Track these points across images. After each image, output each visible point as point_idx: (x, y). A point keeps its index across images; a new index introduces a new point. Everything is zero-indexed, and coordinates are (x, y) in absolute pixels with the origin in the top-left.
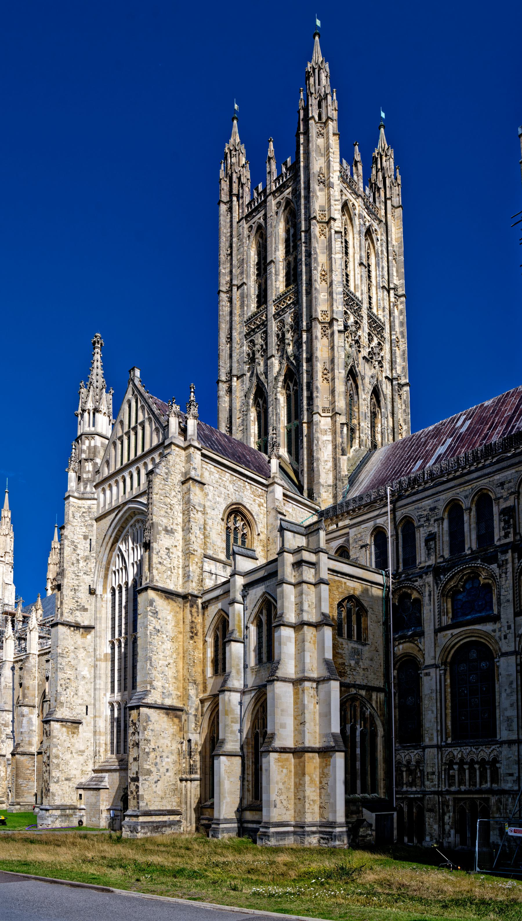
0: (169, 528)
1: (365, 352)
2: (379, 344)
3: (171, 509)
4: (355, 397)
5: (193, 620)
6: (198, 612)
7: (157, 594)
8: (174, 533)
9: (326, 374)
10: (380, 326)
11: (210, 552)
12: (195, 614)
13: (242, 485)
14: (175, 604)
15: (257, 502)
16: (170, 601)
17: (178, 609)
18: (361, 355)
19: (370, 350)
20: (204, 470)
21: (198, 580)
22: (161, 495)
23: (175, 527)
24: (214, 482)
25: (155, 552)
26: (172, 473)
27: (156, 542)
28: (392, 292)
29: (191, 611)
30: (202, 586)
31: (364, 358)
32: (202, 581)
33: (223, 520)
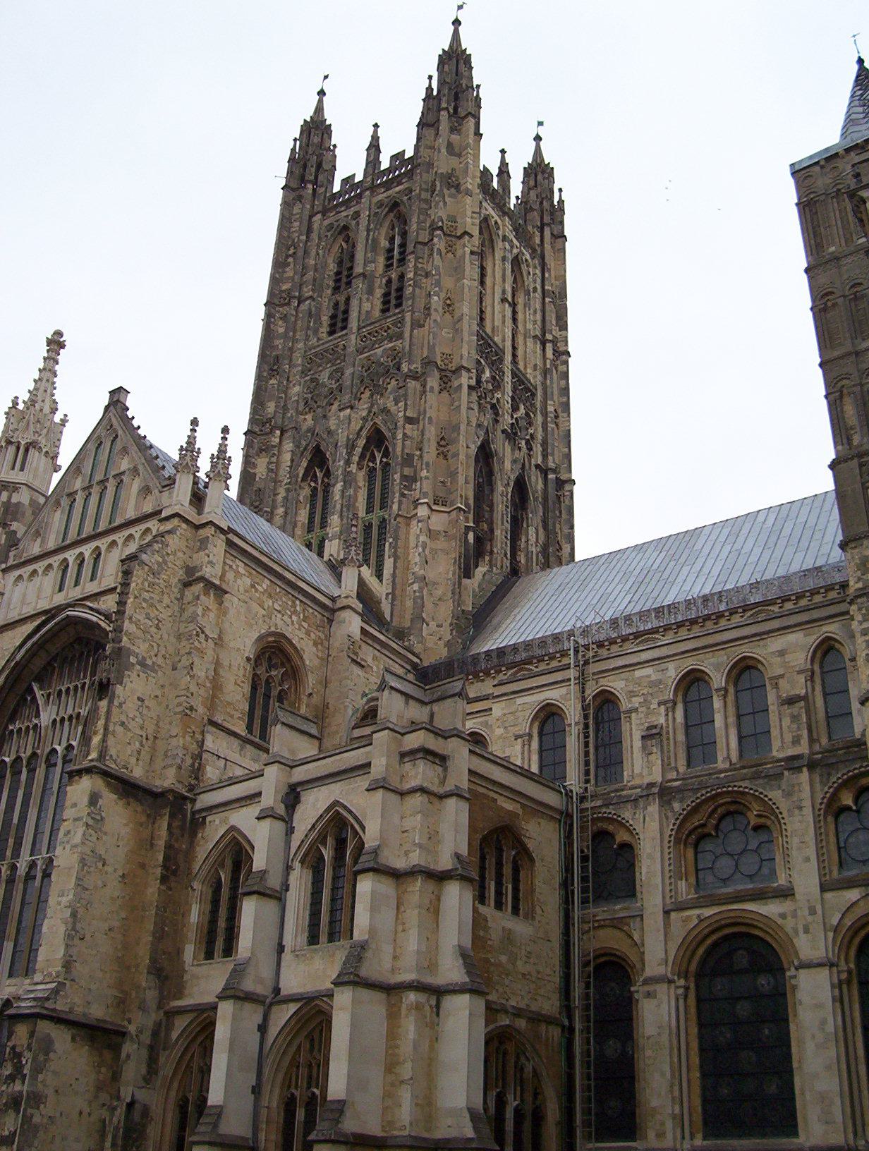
0: (149, 662)
1: (507, 420)
2: (527, 414)
3: (158, 628)
4: (487, 489)
5: (173, 842)
6: (182, 828)
7: (108, 785)
8: (156, 672)
9: (444, 446)
10: (530, 391)
11: (218, 719)
12: (177, 831)
13: (290, 603)
14: (139, 809)
15: (313, 636)
16: (131, 800)
17: (144, 819)
18: (500, 427)
19: (514, 421)
20: (227, 568)
21: (192, 766)
22: (144, 600)
23: (160, 661)
24: (242, 589)
25: (116, 703)
26: (170, 565)
27: (121, 684)
28: (549, 346)
29: (170, 825)
30: (197, 778)
31: (504, 431)
32: (199, 769)
33: (248, 659)
